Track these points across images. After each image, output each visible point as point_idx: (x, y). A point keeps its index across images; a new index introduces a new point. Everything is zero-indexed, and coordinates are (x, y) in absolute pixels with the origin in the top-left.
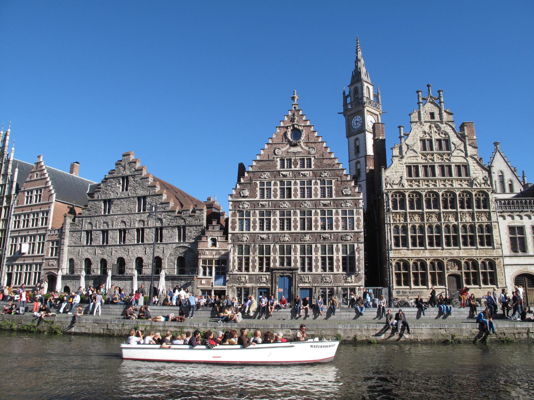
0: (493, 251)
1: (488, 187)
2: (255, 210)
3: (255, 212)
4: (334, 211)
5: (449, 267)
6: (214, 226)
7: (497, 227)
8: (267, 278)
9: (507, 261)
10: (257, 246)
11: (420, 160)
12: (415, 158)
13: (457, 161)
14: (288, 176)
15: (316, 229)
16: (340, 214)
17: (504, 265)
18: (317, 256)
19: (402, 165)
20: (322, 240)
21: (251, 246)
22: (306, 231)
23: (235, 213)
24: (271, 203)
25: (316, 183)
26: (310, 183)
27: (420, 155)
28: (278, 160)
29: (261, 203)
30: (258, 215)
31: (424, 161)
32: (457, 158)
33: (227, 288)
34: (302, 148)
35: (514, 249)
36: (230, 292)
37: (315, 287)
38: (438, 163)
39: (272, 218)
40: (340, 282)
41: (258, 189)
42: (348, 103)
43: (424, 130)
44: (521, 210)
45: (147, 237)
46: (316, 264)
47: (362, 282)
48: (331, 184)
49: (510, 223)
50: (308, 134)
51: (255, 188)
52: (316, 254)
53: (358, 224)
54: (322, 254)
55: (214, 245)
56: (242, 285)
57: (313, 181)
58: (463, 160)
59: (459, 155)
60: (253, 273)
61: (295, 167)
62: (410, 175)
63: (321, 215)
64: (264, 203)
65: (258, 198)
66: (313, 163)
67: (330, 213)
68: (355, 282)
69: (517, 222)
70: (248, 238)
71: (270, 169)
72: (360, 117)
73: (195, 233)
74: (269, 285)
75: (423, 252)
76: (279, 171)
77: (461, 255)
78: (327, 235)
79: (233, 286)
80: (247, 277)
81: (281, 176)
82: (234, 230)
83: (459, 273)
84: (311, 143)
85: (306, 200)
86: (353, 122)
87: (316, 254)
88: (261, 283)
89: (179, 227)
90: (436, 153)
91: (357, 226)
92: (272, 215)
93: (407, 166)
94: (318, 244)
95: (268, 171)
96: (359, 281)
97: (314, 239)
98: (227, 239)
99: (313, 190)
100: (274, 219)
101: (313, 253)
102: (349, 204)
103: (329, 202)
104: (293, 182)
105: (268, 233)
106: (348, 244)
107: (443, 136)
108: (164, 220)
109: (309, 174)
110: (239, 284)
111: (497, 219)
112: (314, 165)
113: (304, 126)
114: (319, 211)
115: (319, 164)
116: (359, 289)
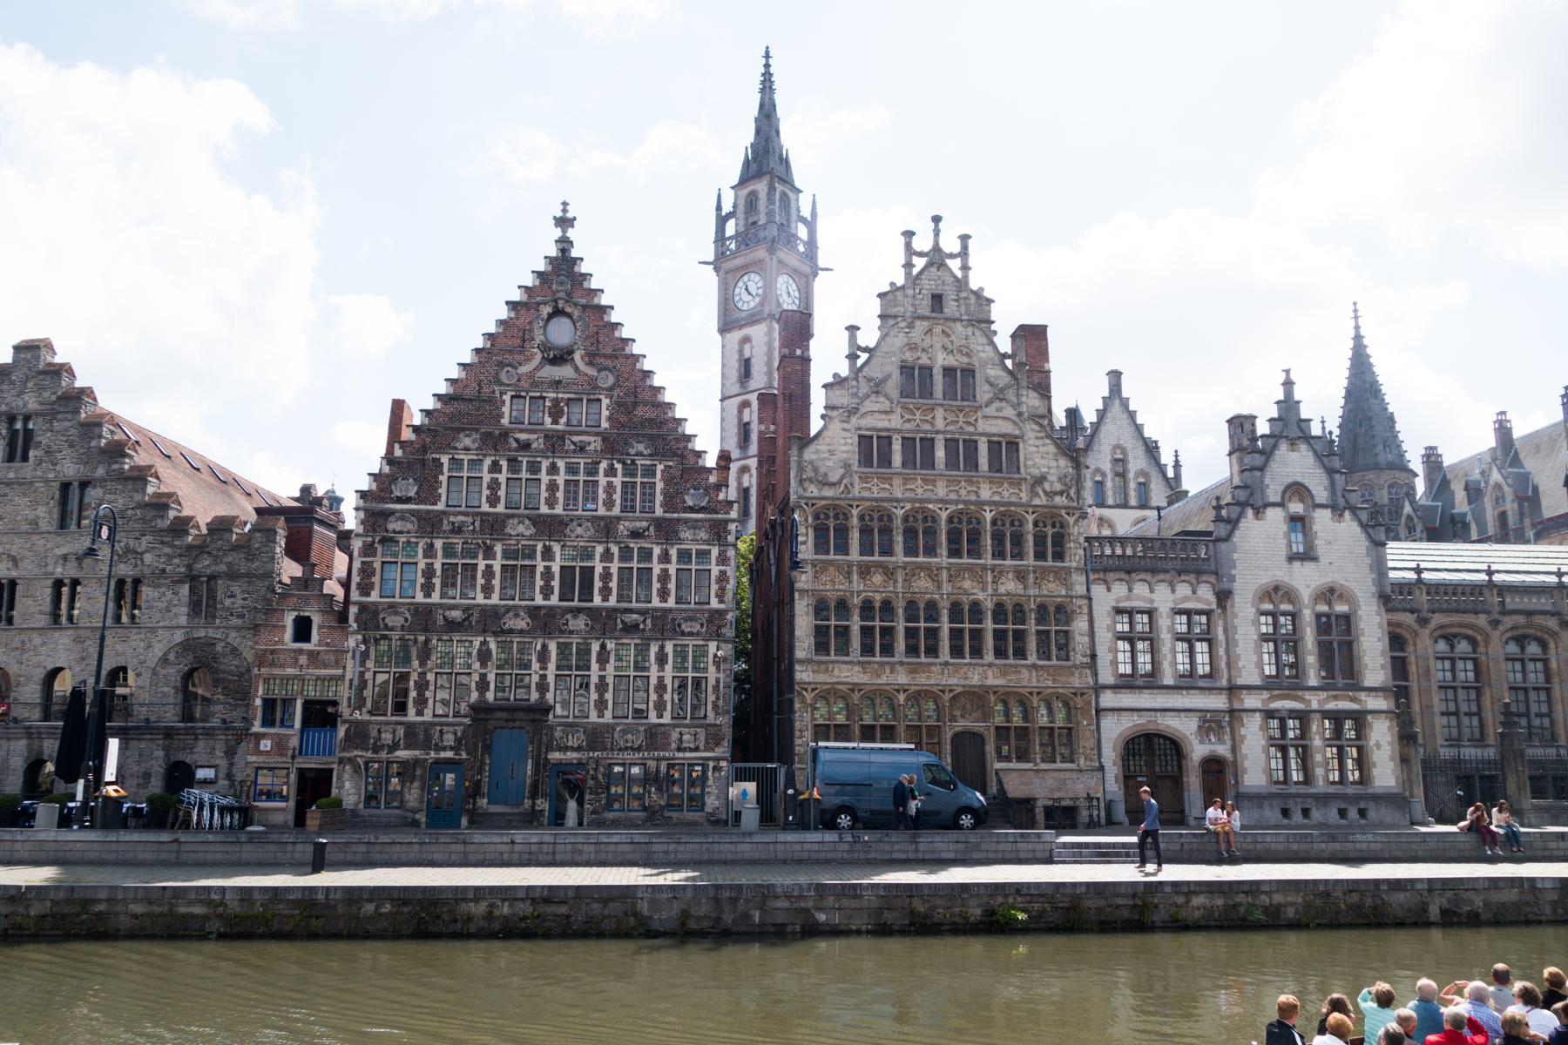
0: (1073, 674)
1: (1071, 504)
3: (432, 545)
4: (657, 551)
5: (958, 713)
7: (1086, 610)
8: (459, 734)
9: (1108, 700)
11: (895, 421)
12: (884, 416)
13: (994, 430)
14: (534, 446)
15: (605, 599)
16: (674, 558)
17: (1097, 712)
18: (603, 673)
19: (848, 434)
20: (622, 630)
21: (416, 641)
22: (575, 603)
24: (482, 521)
25: (611, 471)
26: (592, 470)
27: (899, 410)
28: (507, 398)
29: (452, 519)
30: (440, 553)
31: (908, 426)
32: (993, 422)
33: (340, 763)
36: (346, 776)
37: (597, 761)
38: (943, 433)
39: (482, 564)
40: (666, 747)
42: (727, 235)
43: (913, 340)
46: (601, 696)
47: (723, 750)
48: (654, 475)
49: (1118, 601)
50: (595, 329)
51: (436, 477)
52: (602, 668)
53: (722, 589)
56: (383, 755)
57: (604, 465)
58: (1008, 428)
59: (1000, 414)
60: (419, 719)
61: (555, 422)
62: (866, 460)
63: (622, 559)
64: (461, 518)
65: (440, 506)
67: (646, 555)
68: (706, 750)
70: (406, 620)
71: (478, 423)
72: (757, 278)
73: (245, 599)
74: (464, 756)
75: (892, 672)
76: (505, 434)
77: (990, 681)
78: (635, 616)
80: (401, 731)
81: (514, 445)
82: (368, 595)
83: (982, 730)
84: (605, 356)
85: (579, 518)
86: (737, 291)
87: (600, 670)
88: (438, 749)
90: (941, 405)
91: (717, 596)
92: (481, 556)
93: (860, 436)
94: (607, 641)
95: (477, 430)
96: (717, 744)
97: (598, 627)
99: (601, 490)
100: (487, 566)
101: (595, 666)
102: (703, 535)
103: (645, 524)
104: (545, 464)
105: (466, 609)
106: (691, 643)
107: (965, 360)
109: (595, 444)
110: (375, 752)
111: (1088, 590)
112: (609, 419)
113: (585, 307)
114: (615, 549)
115: (623, 419)
116: (715, 768)
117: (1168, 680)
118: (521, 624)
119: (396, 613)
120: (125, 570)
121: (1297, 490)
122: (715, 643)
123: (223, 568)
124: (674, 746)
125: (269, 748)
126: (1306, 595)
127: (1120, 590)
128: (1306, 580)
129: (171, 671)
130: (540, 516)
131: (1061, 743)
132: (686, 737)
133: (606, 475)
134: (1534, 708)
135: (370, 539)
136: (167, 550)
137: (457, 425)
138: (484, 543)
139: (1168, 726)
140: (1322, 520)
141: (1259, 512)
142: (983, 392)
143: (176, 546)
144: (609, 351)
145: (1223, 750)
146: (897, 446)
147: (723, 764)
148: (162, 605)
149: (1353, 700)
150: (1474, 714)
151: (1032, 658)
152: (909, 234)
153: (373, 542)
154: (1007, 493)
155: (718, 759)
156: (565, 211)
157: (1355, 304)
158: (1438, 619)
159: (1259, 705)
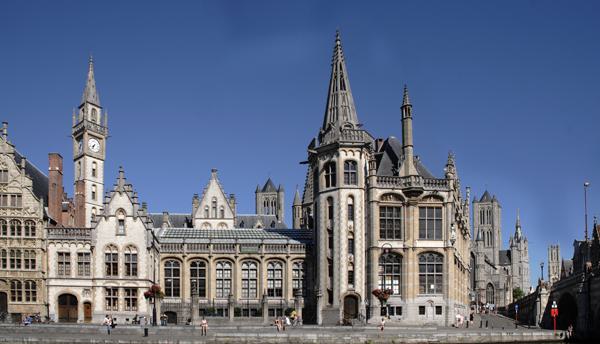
9: (52, 282)
35: (60, 272)
58: (18, 191)
69: (65, 248)
117: (73, 277)
121: (122, 210)
126: (121, 247)
127: (59, 246)
128: (121, 242)
131: (32, 295)
134: (251, 286)
141: (106, 218)
142: (10, 179)
145: (90, 299)
150: (376, 293)
151: (23, 269)
154: (17, 214)
158: (215, 256)
159: (101, 284)
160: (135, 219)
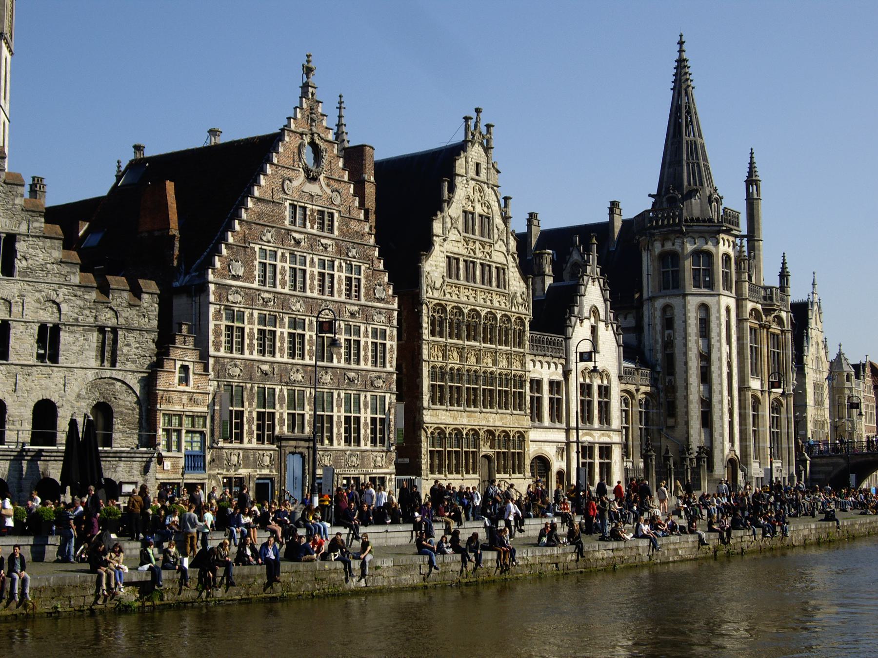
2: (252, 309)
6: (185, 336)
10: (256, 388)
14: (302, 244)
23: (219, 311)
28: (287, 204)
34: (321, 187)
39: (278, 331)
40: (368, 466)
41: (256, 263)
44: (543, 353)
45: (17, 347)
51: (252, 261)
54: (346, 411)
55: (184, 380)
65: (256, 285)
66: (336, 224)
68: (386, 468)
71: (274, 222)
74: (275, 473)
79: (218, 474)
84: (335, 180)
88: (263, 467)
89: (101, 330)
98: (206, 369)
105: (272, 363)
107: (486, 210)
108: (64, 307)
112: (338, 228)
118: (299, 377)
119: (236, 365)
120: (49, 317)
122: (389, 395)
123: (122, 321)
124: (372, 464)
125: (169, 468)
129: (83, 404)
130: (307, 297)
132: (379, 459)
133: (338, 271)
135: (218, 307)
136: (80, 302)
137: (261, 222)
138: (279, 316)
139: (546, 451)
140: (601, 326)
143: (86, 300)
144: (337, 178)
146: (462, 265)
147: (393, 476)
148: (76, 349)
149: (609, 436)
152: (467, 119)
153: (220, 309)
155: (391, 474)
156: (308, 62)
157: (340, 96)
160: (607, 325)
